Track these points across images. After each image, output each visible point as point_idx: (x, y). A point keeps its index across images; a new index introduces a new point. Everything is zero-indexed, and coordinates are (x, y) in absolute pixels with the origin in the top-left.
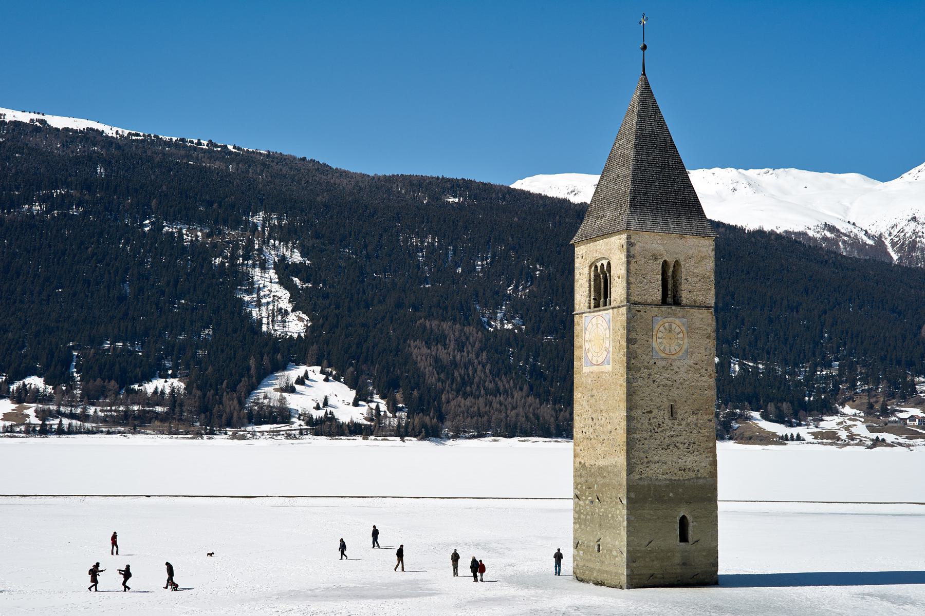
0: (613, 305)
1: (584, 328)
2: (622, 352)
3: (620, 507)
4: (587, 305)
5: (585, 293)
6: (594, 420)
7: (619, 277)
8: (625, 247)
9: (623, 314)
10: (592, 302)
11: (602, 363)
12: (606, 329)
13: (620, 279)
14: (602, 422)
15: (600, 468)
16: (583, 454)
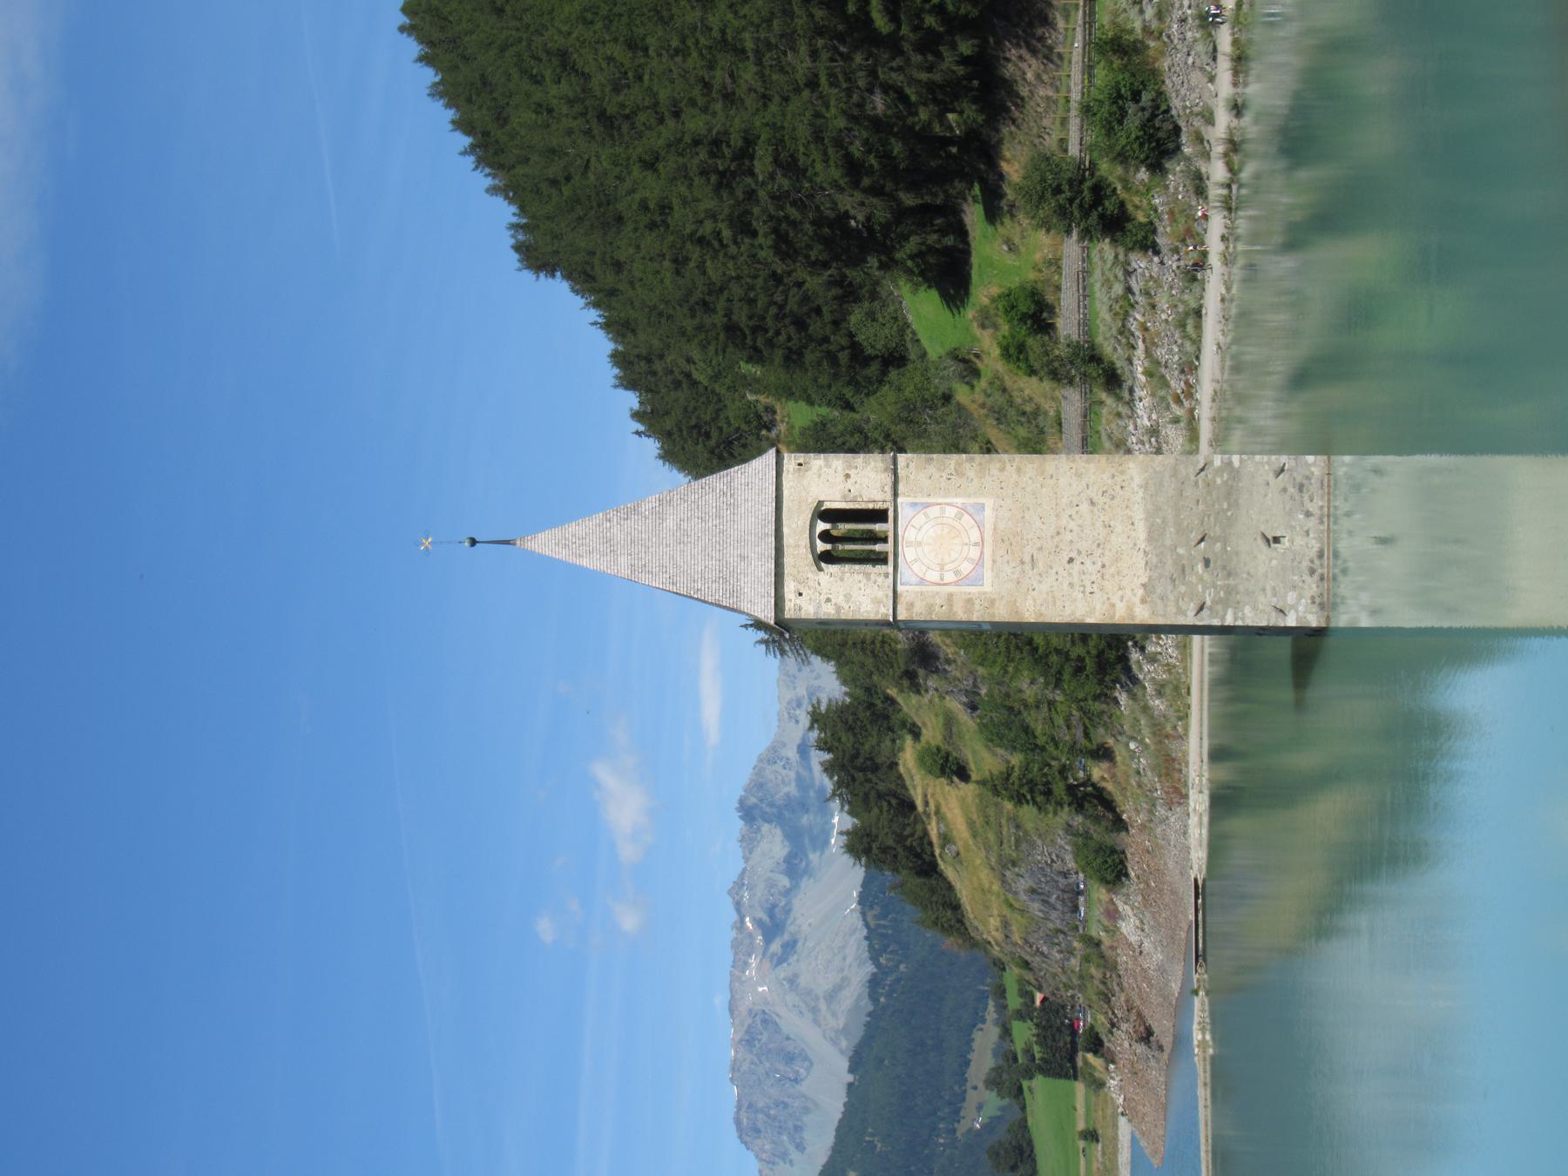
0: (889, 506)
1: (917, 588)
2: (967, 465)
3: (1209, 472)
4: (880, 580)
5: (862, 585)
6: (1073, 555)
7: (848, 476)
8: (801, 457)
9: (908, 466)
10: (880, 568)
11: (980, 525)
12: (926, 515)
13: (852, 472)
14: (1076, 529)
15: (1150, 539)
16: (1128, 592)
